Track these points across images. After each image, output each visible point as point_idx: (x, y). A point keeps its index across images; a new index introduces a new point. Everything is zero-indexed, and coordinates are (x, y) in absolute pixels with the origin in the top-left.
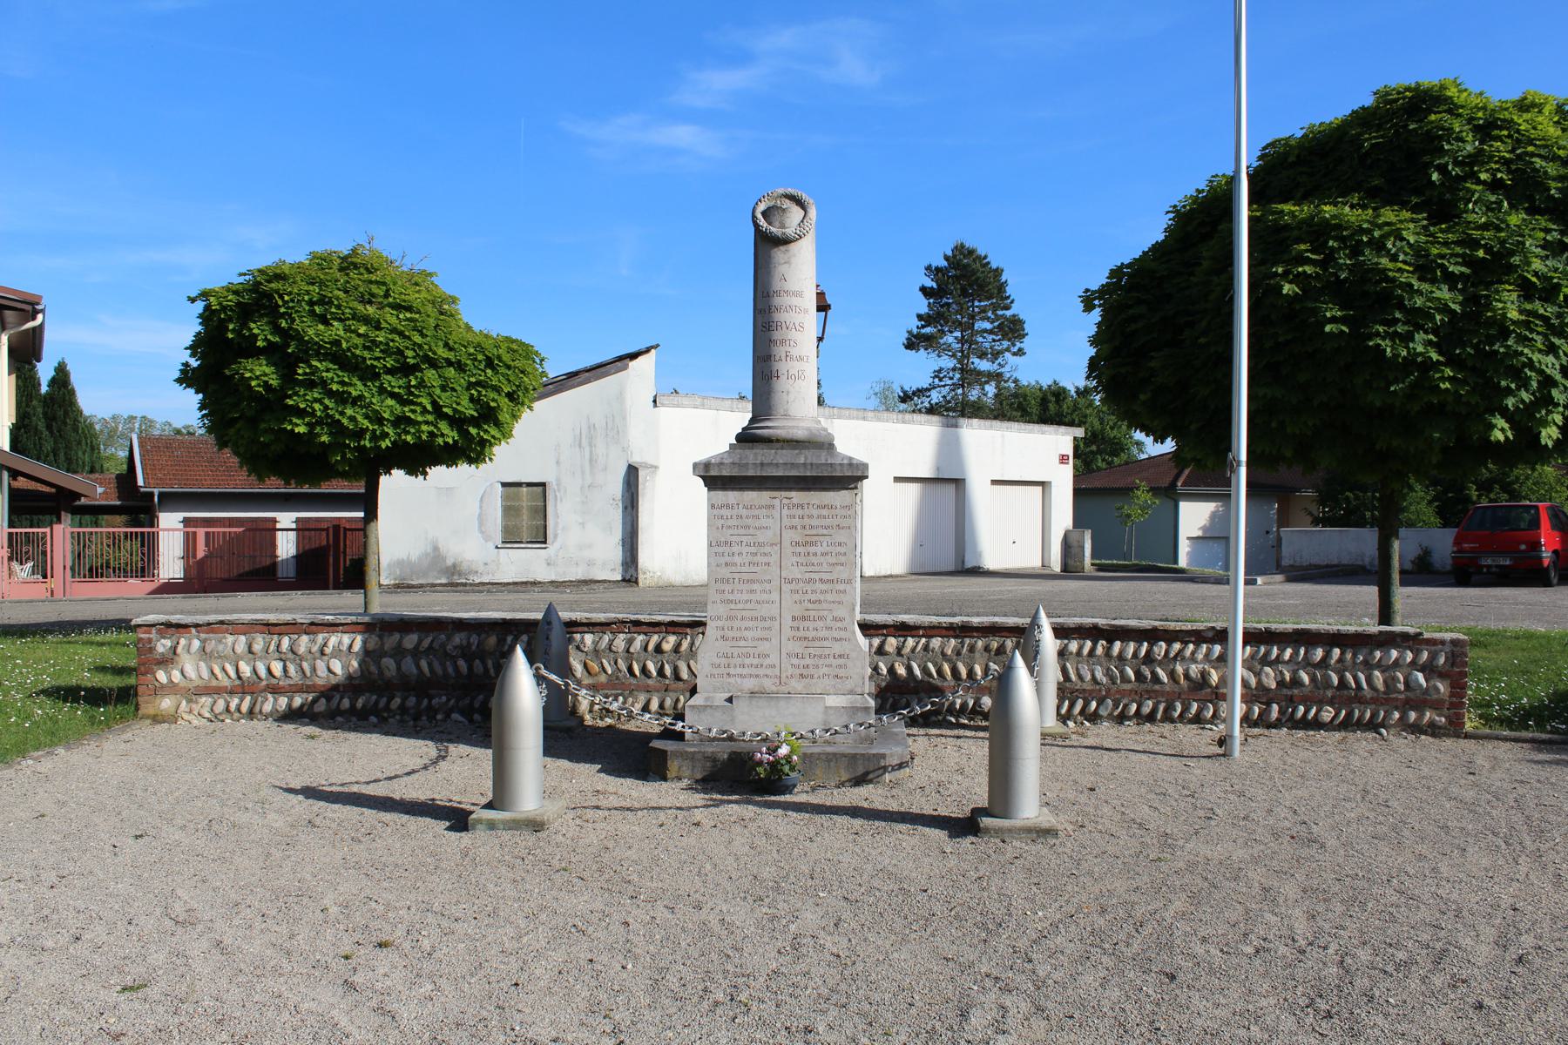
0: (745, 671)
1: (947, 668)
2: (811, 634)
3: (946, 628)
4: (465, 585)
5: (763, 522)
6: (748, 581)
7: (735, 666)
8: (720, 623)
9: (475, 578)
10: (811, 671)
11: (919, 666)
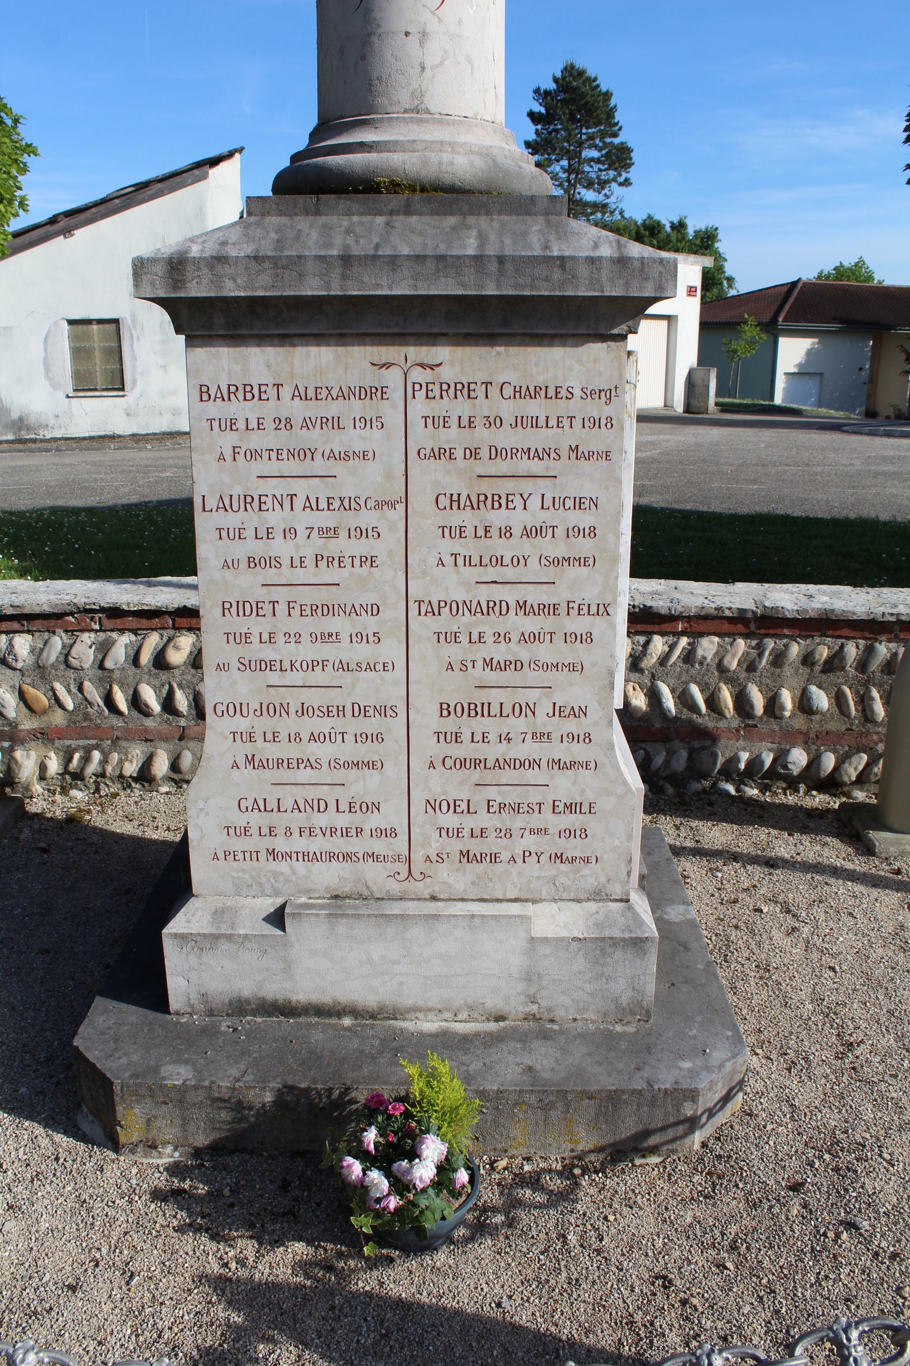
0: (317, 844)
1: (726, 696)
2: (493, 751)
3: (730, 620)
4: (34, 441)
5: (354, 439)
6: (314, 609)
7: (288, 832)
8: (241, 724)
9: (46, 433)
10: (492, 844)
11: (673, 691)
